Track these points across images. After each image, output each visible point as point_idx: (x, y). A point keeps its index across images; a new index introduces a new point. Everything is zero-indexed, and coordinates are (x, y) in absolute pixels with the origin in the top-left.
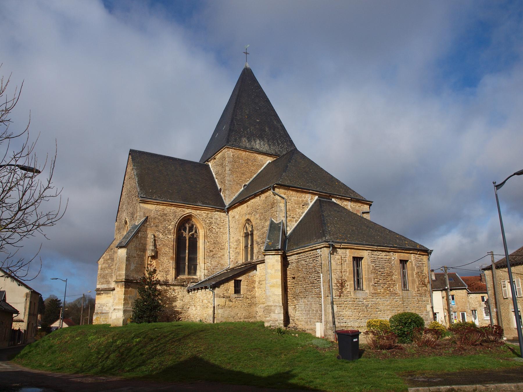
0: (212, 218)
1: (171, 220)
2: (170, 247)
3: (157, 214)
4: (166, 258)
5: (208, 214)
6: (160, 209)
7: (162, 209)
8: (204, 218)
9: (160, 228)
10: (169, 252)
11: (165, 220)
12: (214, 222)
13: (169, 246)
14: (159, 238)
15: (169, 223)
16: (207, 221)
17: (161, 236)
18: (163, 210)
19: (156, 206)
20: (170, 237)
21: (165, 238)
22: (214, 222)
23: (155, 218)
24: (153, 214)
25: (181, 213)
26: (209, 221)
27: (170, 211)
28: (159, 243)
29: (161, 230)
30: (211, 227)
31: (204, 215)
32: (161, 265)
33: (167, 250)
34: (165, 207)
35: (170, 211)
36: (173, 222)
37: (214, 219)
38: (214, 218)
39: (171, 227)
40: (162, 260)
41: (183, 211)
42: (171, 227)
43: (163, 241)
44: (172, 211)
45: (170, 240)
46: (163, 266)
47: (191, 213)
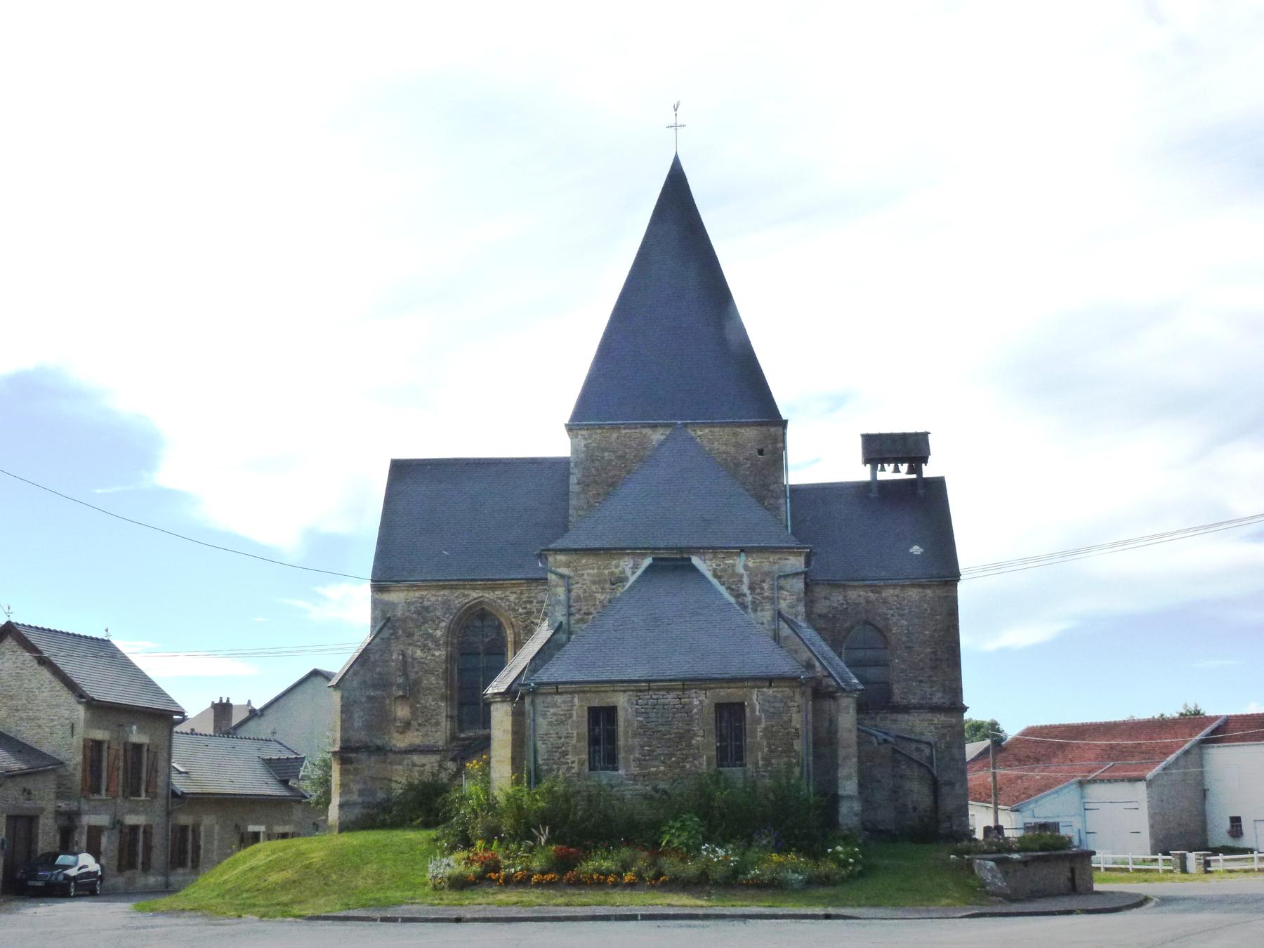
0: (531, 602)
1: (438, 618)
2: (438, 675)
3: (409, 611)
4: (430, 697)
5: (521, 593)
6: (414, 600)
7: (420, 598)
8: (513, 605)
9: (416, 637)
10: (437, 686)
11: (425, 622)
12: (537, 609)
13: (436, 673)
14: (416, 659)
15: (434, 626)
16: (520, 610)
17: (419, 653)
18: (421, 601)
19: (406, 593)
20: (437, 653)
21: (429, 658)
22: (535, 610)
23: (404, 620)
24: (401, 612)
25: (460, 600)
26: (523, 608)
27: (437, 600)
28: (416, 669)
29: (419, 641)
30: (529, 621)
31: (512, 598)
32: (423, 713)
33: (434, 682)
34: (424, 593)
35: (437, 600)
36: (444, 621)
37: (537, 603)
38: (535, 601)
39: (439, 633)
40: (423, 701)
41: (465, 596)
42: (439, 633)
43: (424, 663)
44: (440, 599)
45: (438, 660)
46: (427, 715)
47: (482, 597)
